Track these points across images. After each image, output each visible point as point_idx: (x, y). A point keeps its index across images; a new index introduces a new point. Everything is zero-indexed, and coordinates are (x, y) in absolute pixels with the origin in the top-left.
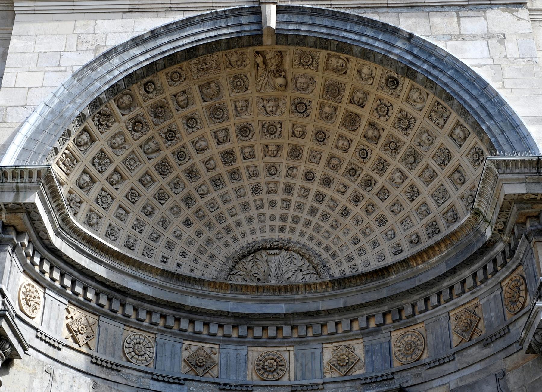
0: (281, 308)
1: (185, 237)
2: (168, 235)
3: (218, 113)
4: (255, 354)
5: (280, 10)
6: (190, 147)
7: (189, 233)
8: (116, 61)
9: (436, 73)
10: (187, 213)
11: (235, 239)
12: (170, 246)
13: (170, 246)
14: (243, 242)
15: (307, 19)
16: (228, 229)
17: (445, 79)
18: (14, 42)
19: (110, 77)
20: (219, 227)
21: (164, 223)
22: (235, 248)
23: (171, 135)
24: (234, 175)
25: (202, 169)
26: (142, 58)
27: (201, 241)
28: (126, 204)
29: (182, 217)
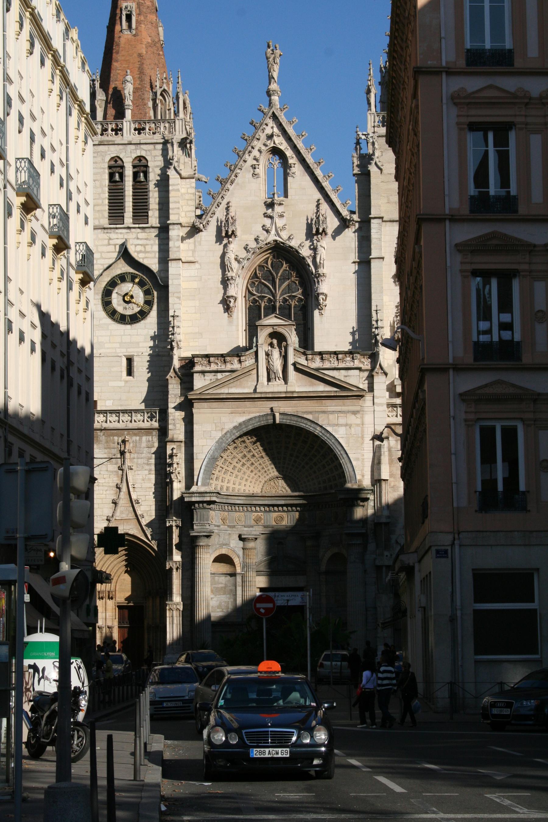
0: (282, 502)
1: (251, 477)
2: (246, 477)
4: (275, 515)
5: (280, 414)
6: (252, 449)
7: (253, 474)
8: (228, 435)
9: (329, 440)
10: (252, 468)
11: (268, 475)
12: (246, 480)
13: (246, 480)
14: (270, 476)
15: (289, 417)
17: (331, 443)
18: (195, 426)
20: (263, 471)
21: (244, 473)
22: (268, 477)
25: (256, 454)
26: (237, 434)
27: (256, 477)
28: (232, 471)
29: (250, 470)
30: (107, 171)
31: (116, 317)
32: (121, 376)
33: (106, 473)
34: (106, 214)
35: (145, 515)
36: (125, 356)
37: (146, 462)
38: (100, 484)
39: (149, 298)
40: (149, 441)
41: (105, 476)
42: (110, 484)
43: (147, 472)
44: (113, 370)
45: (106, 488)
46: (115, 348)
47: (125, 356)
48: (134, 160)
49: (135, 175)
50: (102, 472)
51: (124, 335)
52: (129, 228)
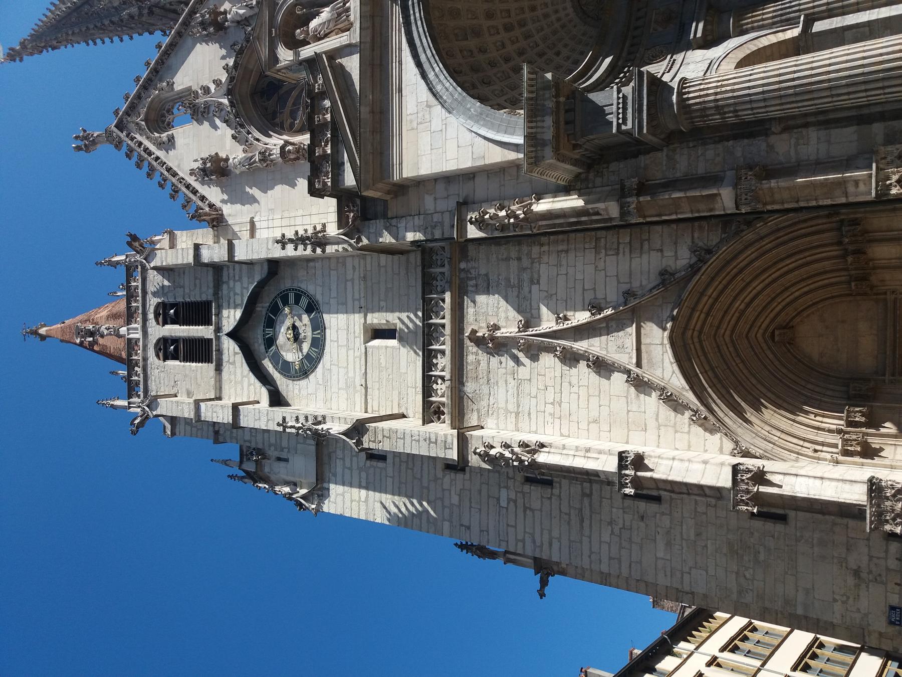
3: (477, 33)
11: (570, 21)
16: (563, 26)
19: (451, 89)
23: (492, 64)
24: (522, 24)
26: (437, 69)
30: (170, 363)
31: (314, 355)
32: (393, 347)
33: (534, 381)
34: (205, 365)
35: (625, 287)
36: (366, 342)
37: (515, 290)
38: (557, 399)
39: (291, 297)
40: (476, 286)
41: (541, 387)
42: (558, 374)
43: (535, 288)
44: (383, 365)
45: (565, 385)
46: (355, 358)
47: (366, 342)
48: (158, 324)
49: (174, 322)
50: (533, 394)
51: (337, 341)
52: (218, 329)
